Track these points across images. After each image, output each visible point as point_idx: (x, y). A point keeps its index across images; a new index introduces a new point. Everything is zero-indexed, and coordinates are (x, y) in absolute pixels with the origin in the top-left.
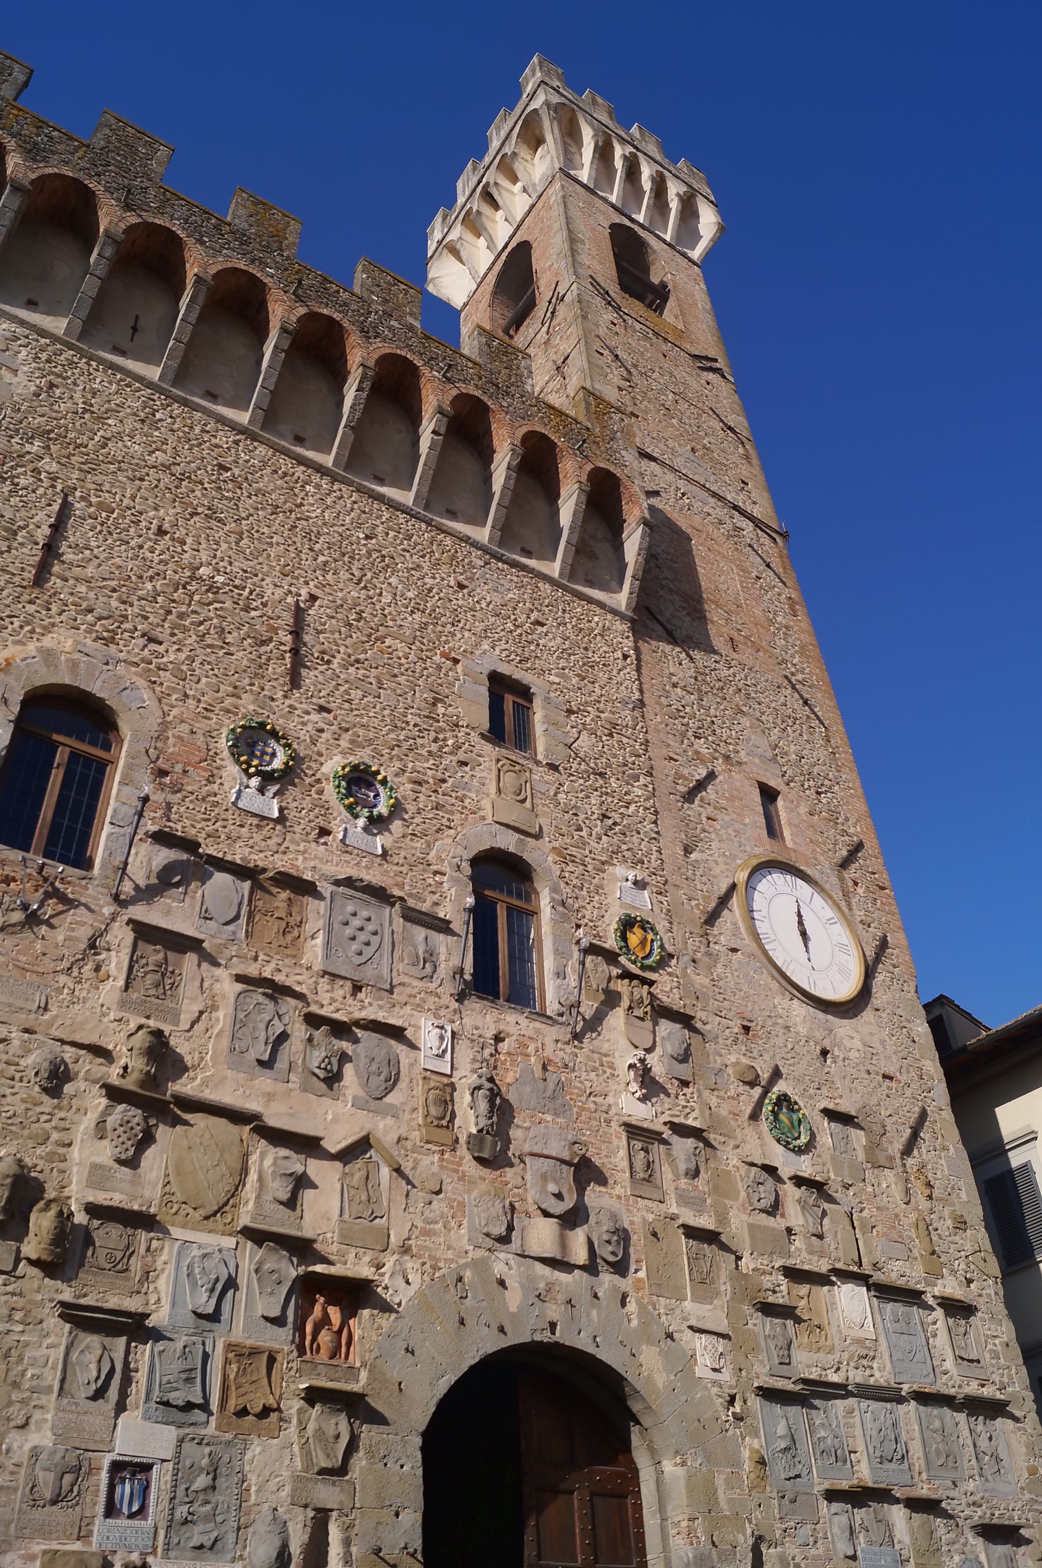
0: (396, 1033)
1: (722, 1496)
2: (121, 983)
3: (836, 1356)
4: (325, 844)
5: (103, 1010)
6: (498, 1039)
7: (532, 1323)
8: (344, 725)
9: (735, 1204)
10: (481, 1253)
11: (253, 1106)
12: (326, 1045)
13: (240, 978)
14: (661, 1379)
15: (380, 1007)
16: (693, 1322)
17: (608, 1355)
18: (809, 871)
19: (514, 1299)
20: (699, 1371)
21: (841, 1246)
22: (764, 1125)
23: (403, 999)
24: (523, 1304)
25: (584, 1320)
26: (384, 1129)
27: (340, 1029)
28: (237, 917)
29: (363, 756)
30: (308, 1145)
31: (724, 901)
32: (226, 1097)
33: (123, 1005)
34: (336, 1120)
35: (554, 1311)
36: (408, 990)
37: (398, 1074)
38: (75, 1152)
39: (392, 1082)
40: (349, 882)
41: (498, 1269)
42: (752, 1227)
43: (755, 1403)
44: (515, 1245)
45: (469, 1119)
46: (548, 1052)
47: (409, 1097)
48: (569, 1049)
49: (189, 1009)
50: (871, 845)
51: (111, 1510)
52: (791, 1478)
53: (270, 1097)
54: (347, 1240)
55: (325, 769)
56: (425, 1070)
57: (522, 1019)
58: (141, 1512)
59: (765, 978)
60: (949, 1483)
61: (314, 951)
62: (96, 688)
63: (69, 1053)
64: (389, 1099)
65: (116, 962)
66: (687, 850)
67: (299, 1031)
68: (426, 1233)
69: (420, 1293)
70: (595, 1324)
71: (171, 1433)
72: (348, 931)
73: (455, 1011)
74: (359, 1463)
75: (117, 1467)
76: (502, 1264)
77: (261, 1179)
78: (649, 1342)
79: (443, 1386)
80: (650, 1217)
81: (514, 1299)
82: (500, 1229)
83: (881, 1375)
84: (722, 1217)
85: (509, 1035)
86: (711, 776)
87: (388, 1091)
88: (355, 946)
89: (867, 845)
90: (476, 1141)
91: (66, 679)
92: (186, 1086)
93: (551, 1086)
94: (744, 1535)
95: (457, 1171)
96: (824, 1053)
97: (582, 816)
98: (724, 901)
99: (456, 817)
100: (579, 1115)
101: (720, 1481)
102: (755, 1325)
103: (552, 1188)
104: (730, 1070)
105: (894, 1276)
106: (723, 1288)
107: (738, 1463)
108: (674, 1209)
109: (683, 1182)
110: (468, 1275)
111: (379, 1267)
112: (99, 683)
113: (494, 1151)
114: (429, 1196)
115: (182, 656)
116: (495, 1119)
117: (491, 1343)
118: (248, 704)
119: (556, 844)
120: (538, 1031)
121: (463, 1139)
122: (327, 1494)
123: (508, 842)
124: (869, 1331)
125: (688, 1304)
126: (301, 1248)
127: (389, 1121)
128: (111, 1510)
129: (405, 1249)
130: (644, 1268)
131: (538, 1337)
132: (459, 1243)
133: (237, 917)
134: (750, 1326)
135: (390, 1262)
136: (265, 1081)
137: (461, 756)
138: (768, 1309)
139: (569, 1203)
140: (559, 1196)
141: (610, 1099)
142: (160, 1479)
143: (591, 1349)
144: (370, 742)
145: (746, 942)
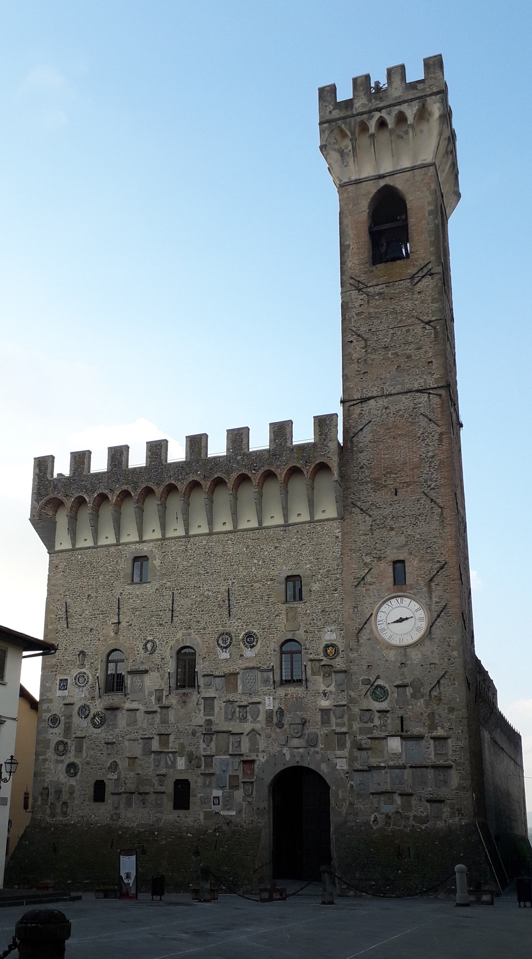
0: (259, 703)
5: (200, 718)
10: (278, 749)
11: (230, 729)
13: (224, 702)
19: (288, 757)
32: (224, 729)
33: (204, 715)
35: (298, 759)
39: (258, 717)
40: (246, 668)
41: (285, 751)
45: (275, 720)
46: (299, 695)
48: (305, 692)
51: (214, 804)
54: (250, 751)
57: (293, 689)
58: (219, 804)
64: (258, 719)
65: (202, 707)
67: (238, 709)
68: (267, 747)
69: (266, 760)
71: (221, 791)
72: (247, 681)
74: (254, 792)
75: (214, 797)
76: (285, 750)
77: (233, 743)
80: (326, 732)
81: (288, 757)
82: (284, 743)
88: (249, 684)
99: (275, 635)
103: (296, 731)
108: (334, 728)
117: (282, 768)
120: (297, 690)
122: (249, 799)
123: (289, 636)
127: (259, 724)
128: (214, 804)
129: (264, 751)
135: (260, 755)
136: (232, 723)
142: (221, 799)
143: (307, 766)
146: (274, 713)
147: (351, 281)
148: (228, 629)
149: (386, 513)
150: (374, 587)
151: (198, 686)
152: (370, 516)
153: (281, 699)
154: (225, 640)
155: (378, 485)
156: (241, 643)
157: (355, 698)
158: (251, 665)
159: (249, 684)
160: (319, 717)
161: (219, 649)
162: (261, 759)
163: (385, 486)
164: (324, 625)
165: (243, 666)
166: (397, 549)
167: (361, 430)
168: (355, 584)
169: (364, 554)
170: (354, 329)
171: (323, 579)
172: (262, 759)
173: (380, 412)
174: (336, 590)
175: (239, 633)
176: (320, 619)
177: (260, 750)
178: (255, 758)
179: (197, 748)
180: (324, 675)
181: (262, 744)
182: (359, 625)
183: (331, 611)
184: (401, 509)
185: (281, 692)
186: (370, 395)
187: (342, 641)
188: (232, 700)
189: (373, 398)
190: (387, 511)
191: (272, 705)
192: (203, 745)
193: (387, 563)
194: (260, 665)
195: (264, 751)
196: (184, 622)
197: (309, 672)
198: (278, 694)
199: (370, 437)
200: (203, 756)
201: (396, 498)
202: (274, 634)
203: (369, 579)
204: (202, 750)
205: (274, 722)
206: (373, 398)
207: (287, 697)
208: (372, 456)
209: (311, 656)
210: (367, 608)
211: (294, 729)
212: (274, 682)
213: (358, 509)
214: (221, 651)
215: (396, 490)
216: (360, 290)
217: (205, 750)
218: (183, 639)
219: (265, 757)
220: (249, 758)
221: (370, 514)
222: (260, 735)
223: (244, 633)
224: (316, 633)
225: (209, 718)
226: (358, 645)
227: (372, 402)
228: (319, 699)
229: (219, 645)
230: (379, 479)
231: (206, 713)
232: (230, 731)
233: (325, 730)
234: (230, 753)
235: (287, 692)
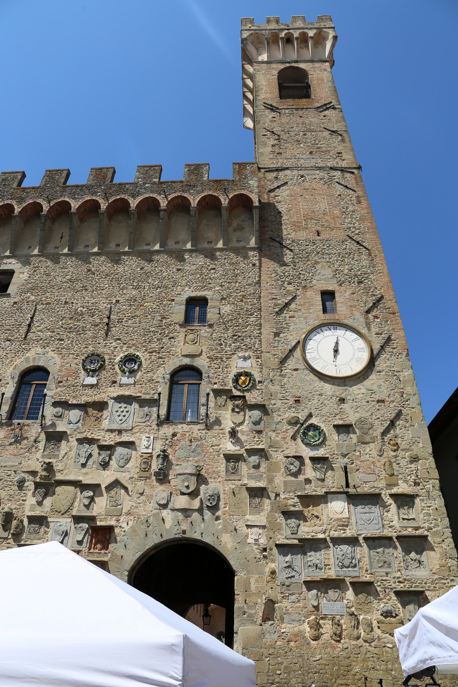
1: (252, 585)
2: (42, 451)
3: (324, 528)
4: (114, 386)
5: (35, 461)
6: (174, 435)
7: (175, 531)
8: (125, 342)
9: (278, 474)
11: (80, 478)
12: (105, 454)
14: (229, 546)
15: (128, 436)
16: (249, 523)
17: (208, 539)
18: (346, 322)
19: (168, 524)
20: (249, 541)
21: (335, 481)
22: (299, 440)
23: (137, 430)
24: (171, 526)
25: (198, 528)
26: (123, 477)
27: (110, 448)
28: (79, 420)
29: (132, 351)
30: (95, 488)
31: (291, 351)
32: (72, 477)
33: (43, 456)
34: (107, 476)
36: (139, 427)
37: (131, 457)
38: (27, 503)
42: (285, 482)
43: (275, 551)
44: (170, 506)
45: (155, 466)
46: (194, 435)
47: (134, 465)
49: (62, 452)
50: (389, 295)
52: (289, 577)
53: (86, 474)
55: (116, 361)
56: (142, 453)
59: (312, 376)
60: (385, 574)
61: (105, 424)
62: (41, 363)
63: (26, 476)
65: (41, 445)
66: (277, 334)
68: (136, 507)
70: (203, 530)
72: (118, 414)
73: (157, 430)
76: (165, 513)
78: (226, 532)
79: (138, 555)
82: (163, 502)
83: (349, 533)
84: (271, 480)
85: (177, 433)
86: (294, 298)
87: (126, 464)
88: (120, 418)
89: (387, 297)
90: (157, 474)
91: (31, 364)
92: (59, 477)
93: (193, 447)
94: (261, 599)
95: (150, 485)
96: (342, 400)
97: (223, 339)
98: (291, 351)
99: (166, 360)
100: (205, 455)
101: (252, 581)
102: (281, 520)
103: (186, 484)
104: (285, 421)
105: (366, 489)
106: (266, 508)
107: (262, 573)
108: (246, 482)
109: (252, 471)
110: (151, 520)
111: (118, 521)
112: (41, 362)
113: (162, 477)
114: (139, 495)
115: (69, 342)
116: (165, 464)
118: (91, 348)
119: (209, 355)
121: (153, 473)
123: (187, 361)
124: (346, 515)
125: (248, 517)
126: (92, 519)
129: (128, 513)
130: (228, 506)
131: (177, 536)
132: (148, 509)
133: (79, 420)
134: (278, 521)
136: (85, 470)
137: (171, 335)
138: (287, 514)
139: (192, 489)
140: (188, 487)
141: (221, 446)
143: (200, 538)
144: (134, 345)
145: (301, 366)
146: (154, 457)
147: (264, 105)
148: (100, 351)
149: (309, 249)
150: (300, 314)
151: (43, 416)
152: (291, 250)
153: (167, 439)
154: (95, 363)
155: (297, 226)
156: (117, 367)
157: (277, 442)
158: (127, 393)
159: (120, 418)
160: (224, 465)
161: (83, 372)
162: (124, 525)
163: (307, 228)
164: (235, 351)
165: (115, 395)
166: (325, 280)
167: (278, 187)
168: (277, 310)
169: (286, 283)
170: (267, 128)
171: (236, 302)
172: (124, 527)
173: (295, 178)
174: (251, 315)
175: (115, 356)
176: (230, 345)
177: (124, 511)
178: (112, 522)
179: (20, 505)
180: (233, 410)
181: (127, 503)
182: (282, 353)
183: (245, 336)
184: (325, 247)
185: (167, 430)
186: (285, 166)
187: (259, 370)
188: (90, 437)
189: (287, 169)
190: (310, 248)
191: (151, 447)
192: (31, 501)
193: (314, 292)
194: (139, 394)
195: (128, 513)
196: (41, 339)
197: (211, 404)
198: (161, 432)
199: (288, 192)
200: (28, 517)
201: (319, 238)
202: (165, 358)
203: (293, 306)
204: (27, 508)
205: (152, 472)
206: (287, 169)
207: (175, 438)
208: (290, 206)
209: (216, 387)
210: (291, 335)
211: (184, 481)
212: (158, 416)
213: (277, 244)
214: (86, 374)
215: (318, 232)
216: (272, 110)
217: (32, 508)
218: (35, 358)
219: (131, 523)
220: (103, 524)
221: (292, 248)
222: (126, 489)
223: (122, 355)
224: (224, 359)
225: (50, 461)
226: (280, 375)
227: (288, 172)
228: (223, 440)
229: (84, 367)
230: (298, 222)
231: (45, 453)
232: (81, 481)
233: (231, 486)
234: (74, 513)
235: (176, 430)
